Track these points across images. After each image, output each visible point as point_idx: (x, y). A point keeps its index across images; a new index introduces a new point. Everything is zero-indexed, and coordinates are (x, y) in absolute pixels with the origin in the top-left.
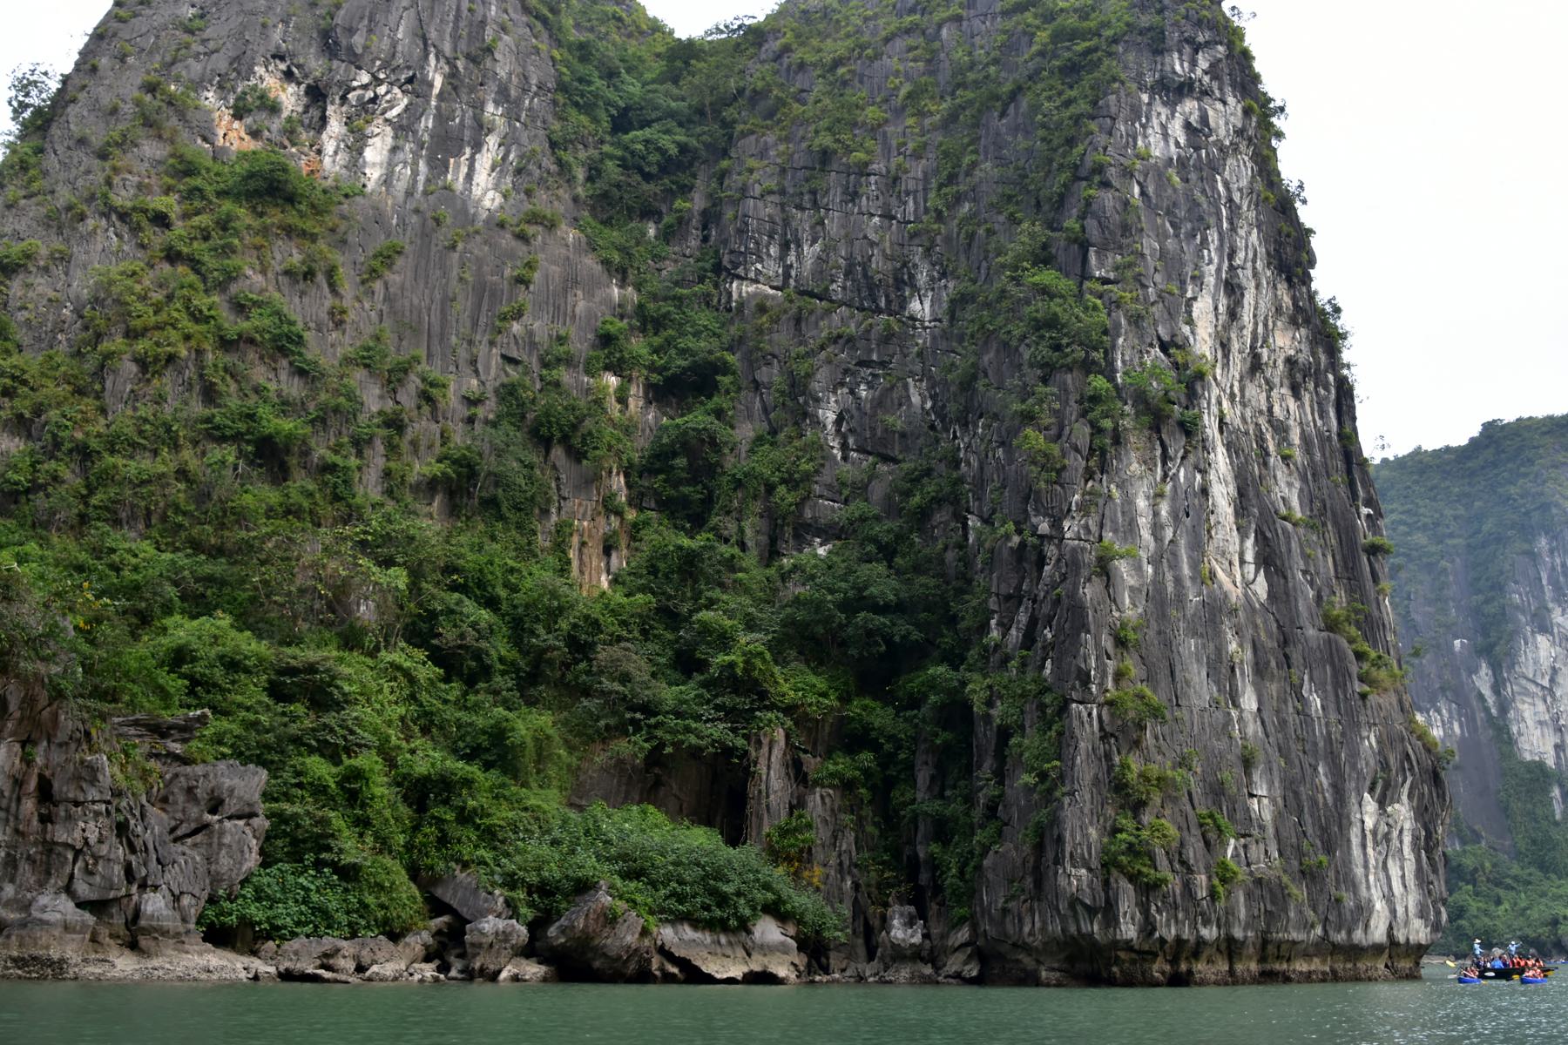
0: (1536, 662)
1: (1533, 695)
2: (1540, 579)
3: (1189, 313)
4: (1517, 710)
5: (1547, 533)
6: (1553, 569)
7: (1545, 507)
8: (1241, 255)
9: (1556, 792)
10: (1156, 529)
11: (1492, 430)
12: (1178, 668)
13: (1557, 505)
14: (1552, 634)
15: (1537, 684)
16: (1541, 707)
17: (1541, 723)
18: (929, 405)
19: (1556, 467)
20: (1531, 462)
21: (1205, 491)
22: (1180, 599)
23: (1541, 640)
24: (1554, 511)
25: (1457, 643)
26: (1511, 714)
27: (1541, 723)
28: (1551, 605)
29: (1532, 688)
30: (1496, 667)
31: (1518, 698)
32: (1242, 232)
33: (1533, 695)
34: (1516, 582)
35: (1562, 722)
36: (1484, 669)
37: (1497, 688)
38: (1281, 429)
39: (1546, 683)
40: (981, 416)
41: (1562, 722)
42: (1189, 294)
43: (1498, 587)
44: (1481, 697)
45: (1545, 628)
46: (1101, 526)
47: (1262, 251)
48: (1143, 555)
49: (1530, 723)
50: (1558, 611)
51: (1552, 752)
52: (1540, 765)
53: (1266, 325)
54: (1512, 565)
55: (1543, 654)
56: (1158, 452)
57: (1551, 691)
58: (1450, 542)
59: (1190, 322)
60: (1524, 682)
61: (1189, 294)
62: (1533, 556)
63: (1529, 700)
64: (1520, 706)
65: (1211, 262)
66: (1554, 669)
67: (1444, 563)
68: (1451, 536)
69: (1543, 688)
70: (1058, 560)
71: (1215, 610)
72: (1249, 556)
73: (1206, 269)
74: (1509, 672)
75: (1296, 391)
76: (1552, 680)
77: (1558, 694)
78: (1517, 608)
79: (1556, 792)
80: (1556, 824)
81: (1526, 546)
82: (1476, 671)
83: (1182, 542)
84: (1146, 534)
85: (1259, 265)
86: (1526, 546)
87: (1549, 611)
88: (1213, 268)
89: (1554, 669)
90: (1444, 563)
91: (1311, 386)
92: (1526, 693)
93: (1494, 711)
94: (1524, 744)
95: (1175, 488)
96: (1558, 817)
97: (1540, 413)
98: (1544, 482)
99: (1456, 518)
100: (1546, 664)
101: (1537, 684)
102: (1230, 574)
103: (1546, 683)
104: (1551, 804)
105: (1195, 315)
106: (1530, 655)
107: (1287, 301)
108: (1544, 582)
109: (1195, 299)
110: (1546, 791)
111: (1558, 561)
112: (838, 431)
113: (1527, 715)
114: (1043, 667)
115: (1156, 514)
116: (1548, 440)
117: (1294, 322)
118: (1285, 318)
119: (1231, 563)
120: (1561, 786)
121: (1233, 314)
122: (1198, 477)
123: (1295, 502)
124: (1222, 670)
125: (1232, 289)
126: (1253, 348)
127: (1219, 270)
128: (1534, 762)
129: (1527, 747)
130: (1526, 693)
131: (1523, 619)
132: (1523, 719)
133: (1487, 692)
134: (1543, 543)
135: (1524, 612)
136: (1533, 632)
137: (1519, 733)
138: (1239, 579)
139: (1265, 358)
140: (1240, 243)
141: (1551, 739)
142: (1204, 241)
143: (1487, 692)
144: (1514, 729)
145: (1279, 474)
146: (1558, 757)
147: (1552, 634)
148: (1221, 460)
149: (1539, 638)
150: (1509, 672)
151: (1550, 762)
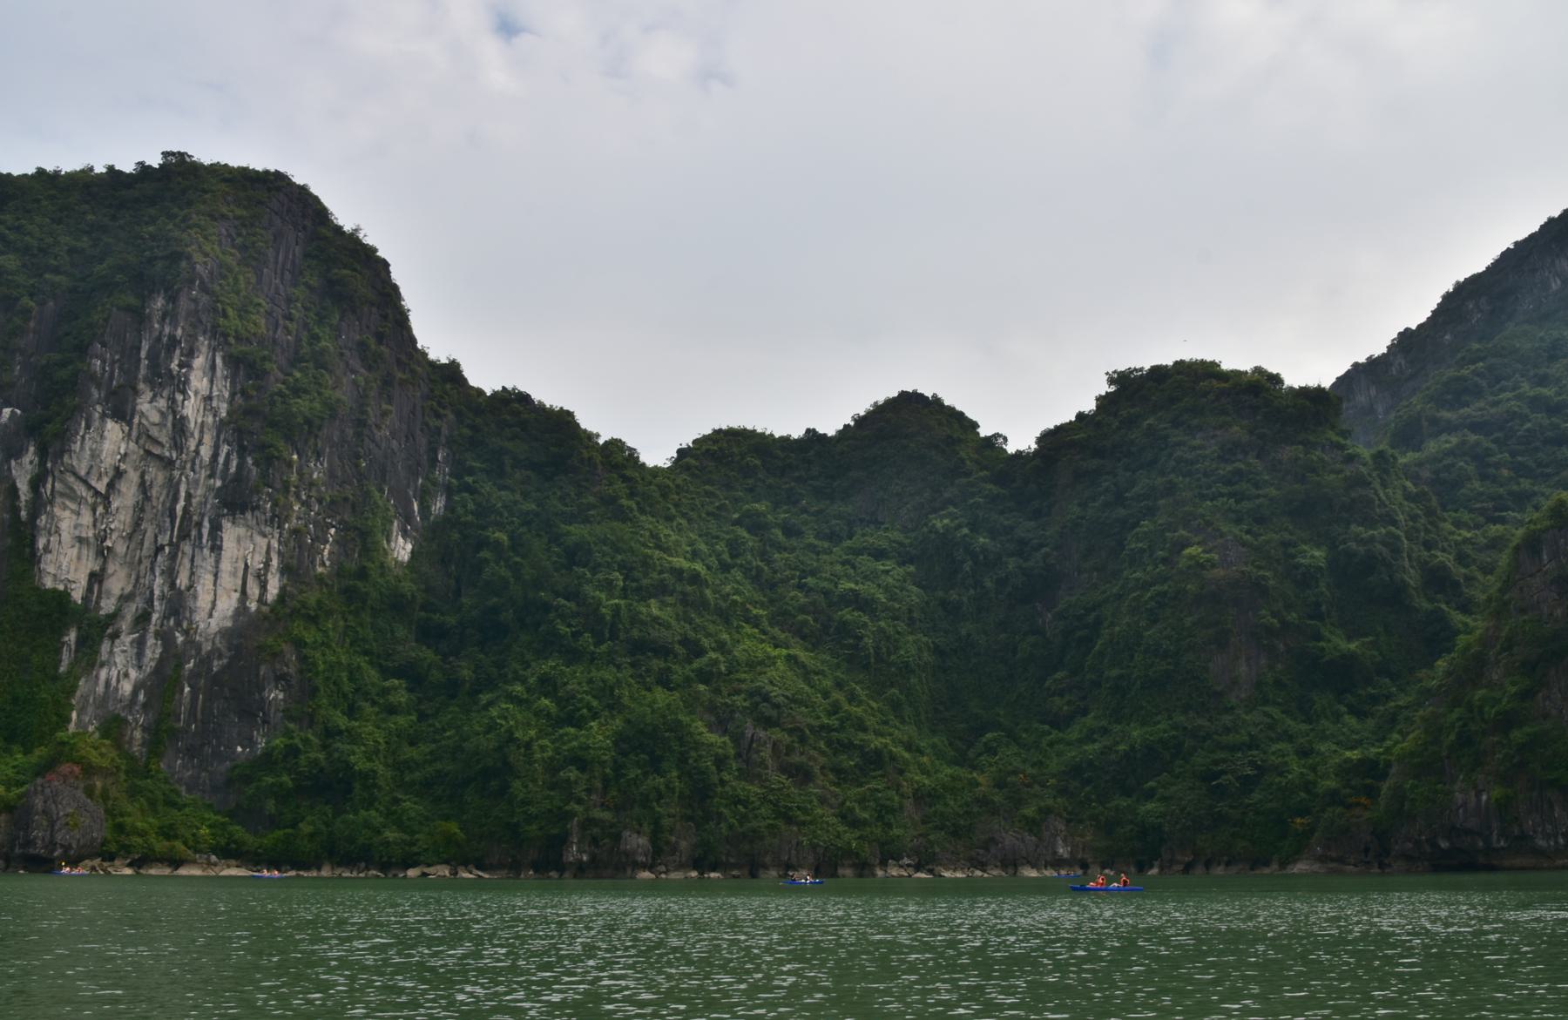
0: (95, 455)
1: (79, 500)
2: (139, 349)
4: (52, 516)
5: (166, 291)
6: (159, 339)
7: (176, 257)
9: (72, 636)
11: (179, 169)
13: (189, 258)
14: (130, 424)
15: (90, 487)
16: (87, 518)
17: (81, 540)
19: (213, 218)
20: (189, 204)
23: (113, 429)
24: (184, 264)
25: (7, 411)
26: (42, 521)
27: (81, 540)
28: (141, 386)
29: (81, 490)
30: (43, 452)
31: (58, 500)
33: (79, 500)
34: (104, 345)
35: (109, 543)
36: (30, 455)
37: (36, 483)
39: (101, 487)
41: (109, 543)
43: (82, 350)
44: (14, 491)
45: (122, 411)
49: (66, 537)
50: (149, 395)
51: (84, 582)
52: (62, 598)
54: (106, 320)
55: (107, 446)
57: (107, 505)
58: (47, 276)
60: (71, 479)
62: (140, 318)
63: (74, 506)
64: (57, 511)
66: (117, 469)
67: (26, 301)
68: (56, 270)
69: (97, 493)
74: (54, 463)
76: (111, 486)
77: (115, 505)
78: (93, 377)
79: (72, 636)
80: (55, 678)
81: (132, 300)
82: (18, 454)
86: (132, 300)
87: (136, 393)
89: (117, 469)
90: (26, 301)
92: (71, 495)
93: (23, 513)
94: (48, 565)
96: (62, 669)
97: (235, 162)
98: (189, 227)
99: (72, 251)
101: (90, 487)
103: (101, 487)
104: (58, 651)
106: (88, 444)
108: (143, 354)
110: (62, 631)
111: (167, 330)
113: (64, 525)
116: (223, 187)
120: (79, 629)
128: (55, 590)
129: (51, 569)
131: (95, 394)
132: (58, 532)
133: (23, 487)
134: (159, 303)
135: (99, 387)
136: (103, 416)
137: (47, 550)
141: (90, 564)
143: (23, 487)
144: (41, 543)
146: (89, 589)
147: (130, 424)
150: (54, 463)
151: (77, 595)
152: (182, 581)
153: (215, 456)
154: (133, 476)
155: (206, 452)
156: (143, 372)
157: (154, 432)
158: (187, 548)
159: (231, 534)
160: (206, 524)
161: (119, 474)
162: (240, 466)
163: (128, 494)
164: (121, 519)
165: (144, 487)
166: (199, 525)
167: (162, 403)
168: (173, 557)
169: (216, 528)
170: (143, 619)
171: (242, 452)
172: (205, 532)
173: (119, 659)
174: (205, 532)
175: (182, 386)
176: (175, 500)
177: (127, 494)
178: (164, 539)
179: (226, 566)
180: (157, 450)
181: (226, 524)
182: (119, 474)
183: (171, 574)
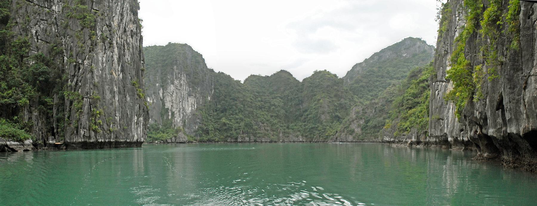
0: (170, 89)
3: (113, 19)
8: (125, 9)
10: (103, 63)
12: (104, 92)
18: (56, 31)
21: (112, 57)
22: (106, 78)
26: (165, 99)
28: (174, 79)
31: (166, 96)
32: (125, 4)
38: (128, 44)
39: (171, 94)
40: (68, 35)
42: (113, 15)
45: (173, 83)
46: (92, 62)
47: (129, 8)
48: (99, 69)
53: (128, 23)
55: (172, 88)
56: (104, 48)
57: (172, 96)
59: (113, 21)
61: (113, 15)
65: (118, 9)
70: (83, 69)
71: (112, 80)
72: (119, 70)
73: (117, 11)
75: (132, 37)
76: (173, 93)
78: (168, 79)
83: (107, 66)
84: (100, 65)
85: (128, 11)
88: (119, 10)
91: (135, 36)
92: (168, 95)
95: (107, 55)
100: (172, 90)
102: (116, 73)
103: (171, 94)
105: (114, 20)
107: (133, 18)
109: (114, 16)
112: (36, 35)
113: (167, 99)
114: (79, 90)
115: (103, 61)
117: (134, 23)
118: (132, 22)
119: (116, 71)
121: (121, 20)
122: (111, 53)
123: (129, 59)
124: (112, 92)
125: (122, 15)
126: (125, 27)
127: (120, 11)
130: (168, 95)
138: (117, 74)
139: (127, 30)
140: (125, 6)
142: (118, 5)
145: (127, 53)
146: (171, 108)
148: (116, 50)
149: (172, 85)
152: (184, 106)
153: (186, 88)
154: (175, 92)
155: (185, 88)
156: (174, 78)
157: (177, 85)
158: (184, 101)
159: (189, 99)
160: (186, 98)
161: (173, 92)
162: (189, 90)
163: (175, 94)
164: (174, 98)
165: (176, 93)
166: (185, 98)
167: (178, 82)
168: (182, 103)
169: (187, 99)
170: (179, 111)
171: (189, 87)
172: (186, 99)
173: (177, 117)
174: (186, 99)
175: (181, 79)
176: (182, 95)
177: (175, 94)
178: (181, 100)
179: (189, 103)
180: (178, 88)
181: (189, 98)
182: (173, 92)
183: (182, 105)
